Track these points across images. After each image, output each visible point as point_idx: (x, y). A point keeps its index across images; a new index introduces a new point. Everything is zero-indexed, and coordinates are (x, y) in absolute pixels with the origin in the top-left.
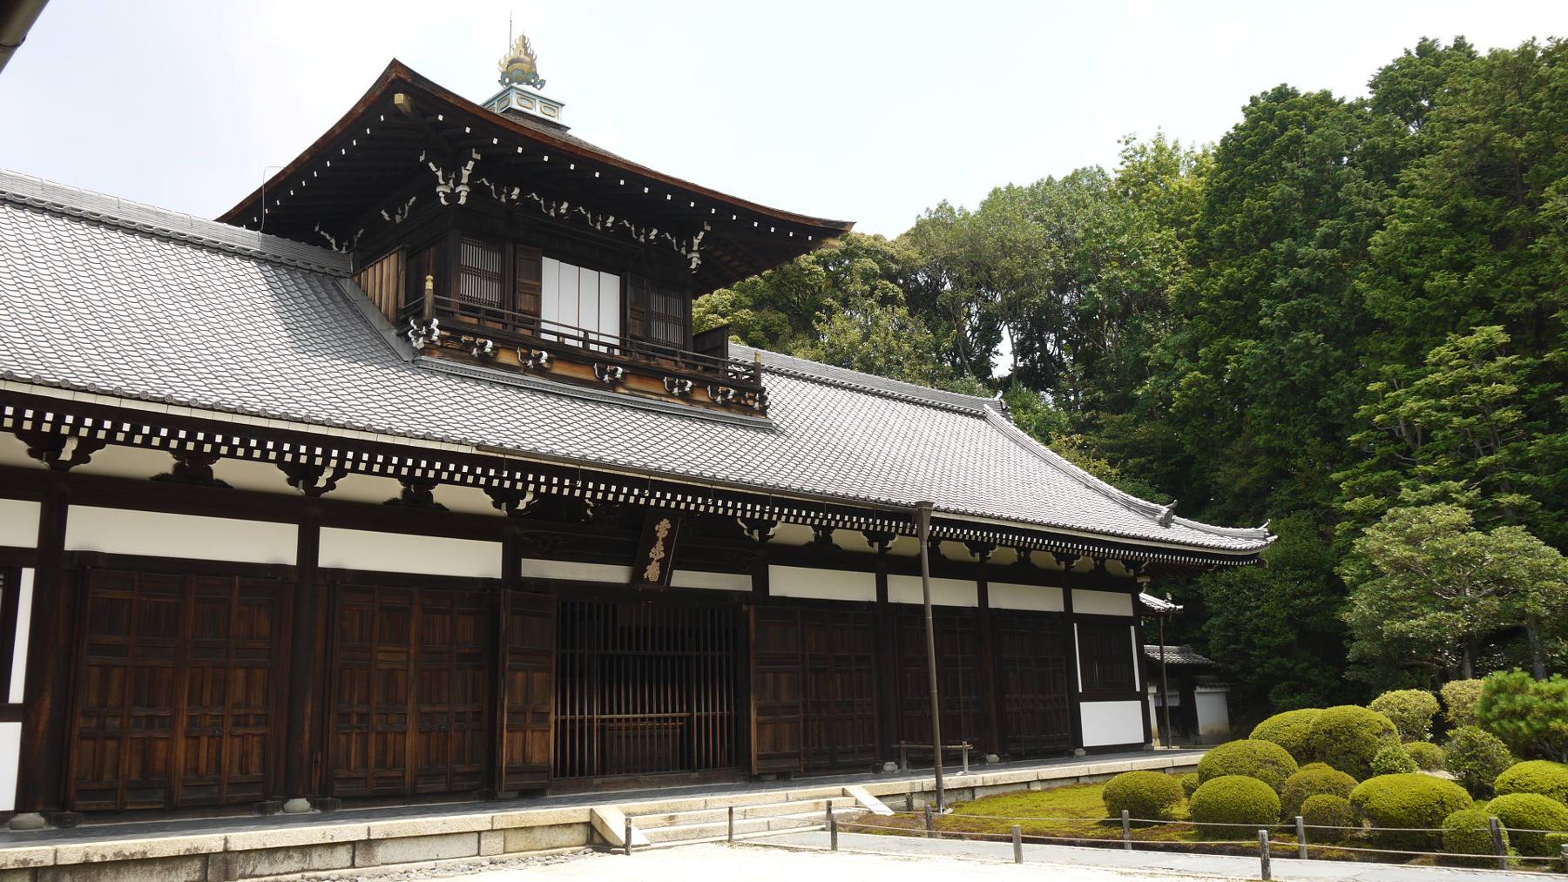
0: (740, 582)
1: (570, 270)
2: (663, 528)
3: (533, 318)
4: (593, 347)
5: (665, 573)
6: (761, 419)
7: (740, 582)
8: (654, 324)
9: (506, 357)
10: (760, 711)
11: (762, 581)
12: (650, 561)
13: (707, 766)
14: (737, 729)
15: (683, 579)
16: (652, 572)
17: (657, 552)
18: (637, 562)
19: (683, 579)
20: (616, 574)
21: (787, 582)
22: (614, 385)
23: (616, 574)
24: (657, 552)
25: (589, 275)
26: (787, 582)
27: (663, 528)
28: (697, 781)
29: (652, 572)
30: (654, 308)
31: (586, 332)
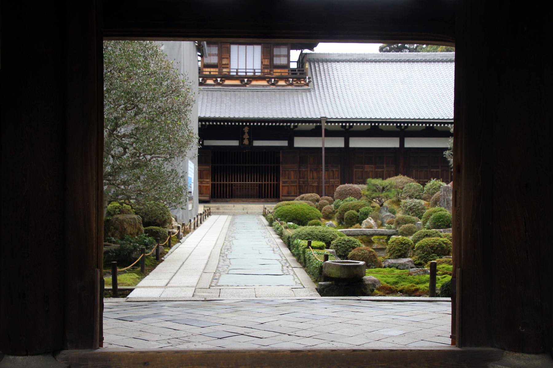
0: (285, 143)
1: (242, 48)
2: (246, 130)
3: (228, 66)
4: (239, 74)
5: (251, 142)
6: (306, 87)
7: (285, 143)
8: (275, 59)
9: (210, 82)
10: (284, 182)
11: (291, 143)
12: (244, 139)
13: (268, 198)
14: (277, 187)
15: (257, 143)
16: (246, 142)
17: (246, 136)
18: (241, 140)
19: (257, 143)
20: (235, 143)
21: (300, 143)
22: (245, 85)
23: (235, 143)
24: (246, 136)
25: (250, 48)
26: (300, 143)
27: (246, 130)
28: (263, 202)
29: (246, 142)
30: (275, 53)
31: (237, 70)
